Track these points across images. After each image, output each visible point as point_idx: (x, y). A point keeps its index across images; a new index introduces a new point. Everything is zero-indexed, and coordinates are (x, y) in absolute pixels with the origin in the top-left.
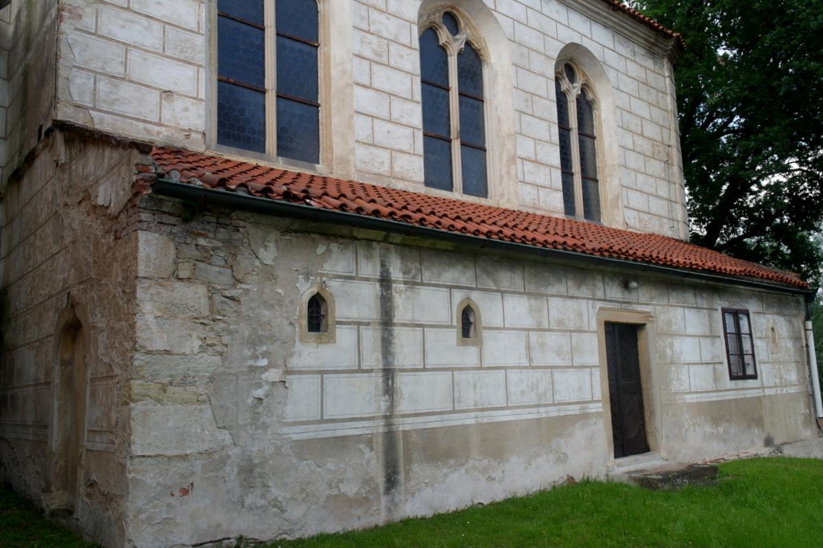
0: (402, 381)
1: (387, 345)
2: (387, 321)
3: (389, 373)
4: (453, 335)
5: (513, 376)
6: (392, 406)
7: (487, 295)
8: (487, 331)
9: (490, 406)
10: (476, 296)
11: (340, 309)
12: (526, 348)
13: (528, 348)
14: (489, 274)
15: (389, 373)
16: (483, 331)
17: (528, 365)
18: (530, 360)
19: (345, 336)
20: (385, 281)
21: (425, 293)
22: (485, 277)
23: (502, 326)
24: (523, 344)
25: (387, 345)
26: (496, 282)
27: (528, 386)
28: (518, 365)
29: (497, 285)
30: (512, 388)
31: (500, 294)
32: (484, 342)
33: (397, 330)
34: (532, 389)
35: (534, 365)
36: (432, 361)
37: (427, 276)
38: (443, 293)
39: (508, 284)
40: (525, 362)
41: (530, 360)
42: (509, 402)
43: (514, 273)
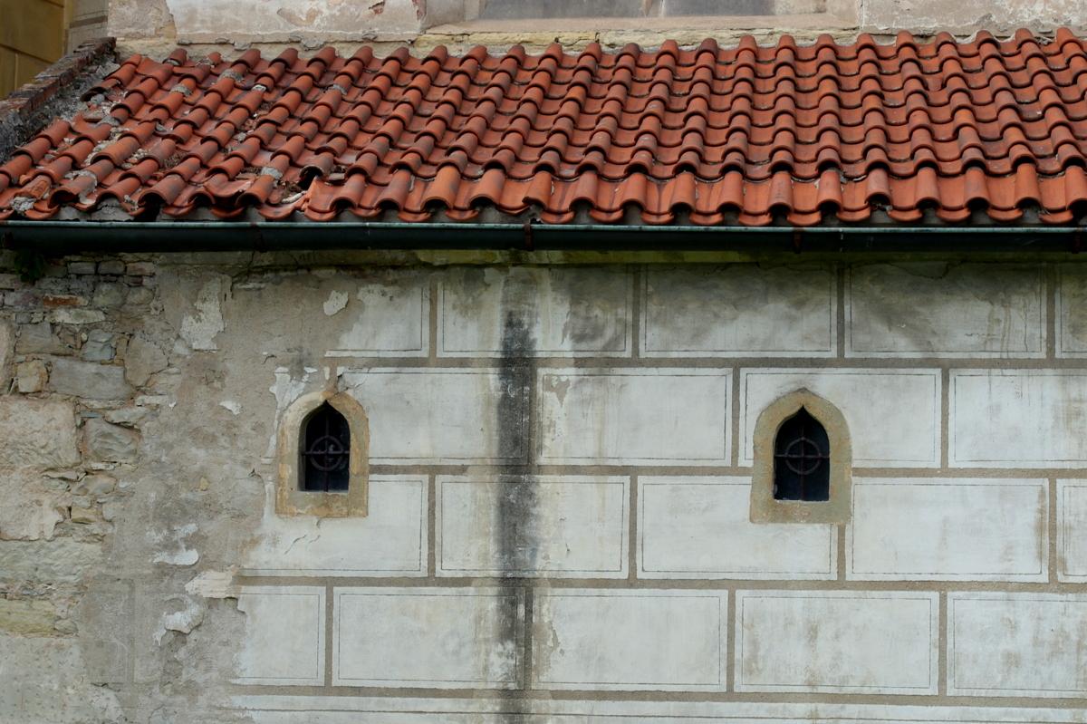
0: (553, 609)
1: (514, 520)
2: (517, 459)
3: (517, 589)
4: (739, 496)
5: (970, 610)
6: (526, 667)
7: (881, 378)
8: (864, 480)
9: (866, 691)
10: (834, 391)
11: (378, 440)
12: (1040, 529)
13: (1049, 526)
14: (891, 318)
15: (517, 589)
16: (855, 480)
17: (1044, 578)
18: (1055, 562)
19: (391, 504)
20: (517, 364)
21: (642, 387)
22: (879, 327)
23: (937, 464)
24: (1026, 518)
25: (514, 520)
26: (919, 336)
27: (1037, 642)
28: (998, 578)
29: (928, 347)
30: (963, 644)
31: (938, 372)
32: (857, 511)
33: (546, 485)
34: (1056, 652)
35: (1070, 580)
36: (654, 561)
37: (653, 339)
38: (714, 382)
39: (973, 340)
40: (1029, 567)
41: (1055, 562)
42: (949, 682)
43: (1006, 304)
